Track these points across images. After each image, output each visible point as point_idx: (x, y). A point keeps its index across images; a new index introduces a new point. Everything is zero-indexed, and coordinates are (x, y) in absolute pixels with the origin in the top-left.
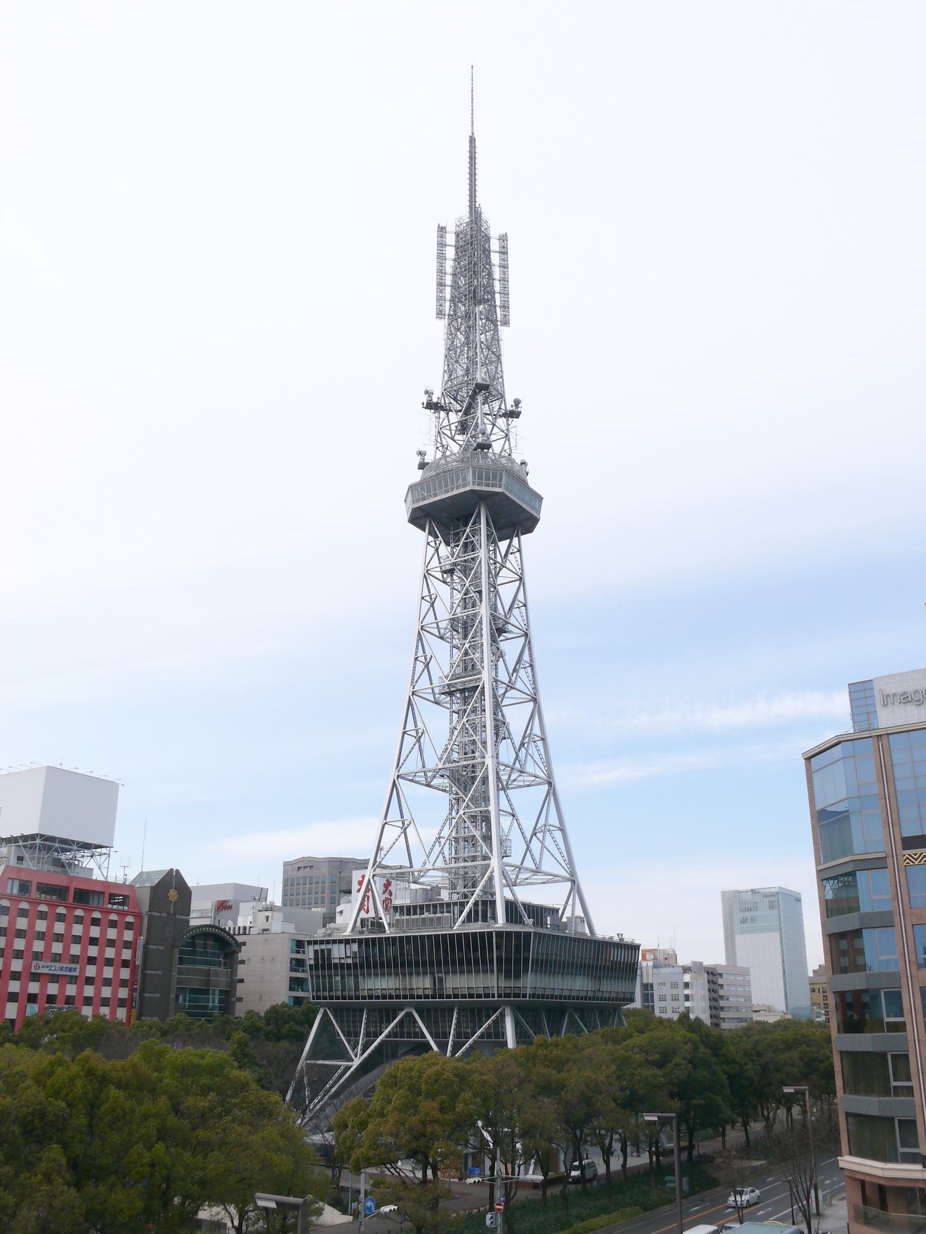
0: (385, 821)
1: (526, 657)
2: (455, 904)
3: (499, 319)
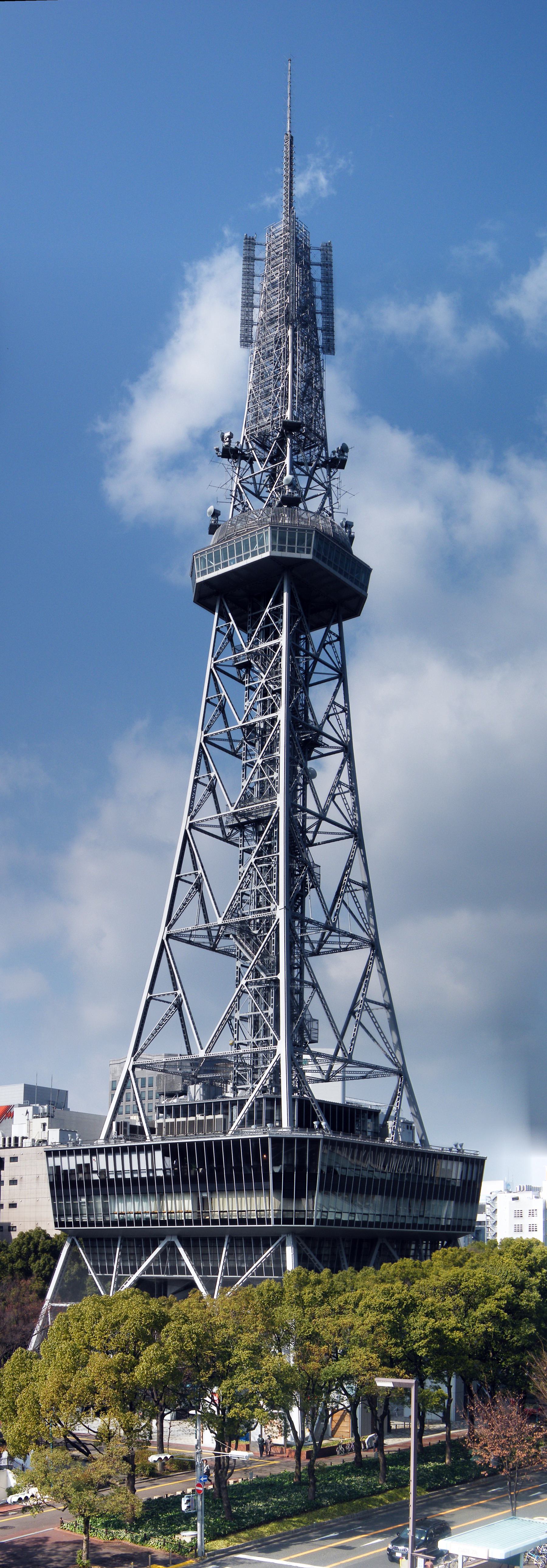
0: (149, 995)
3: (320, 344)
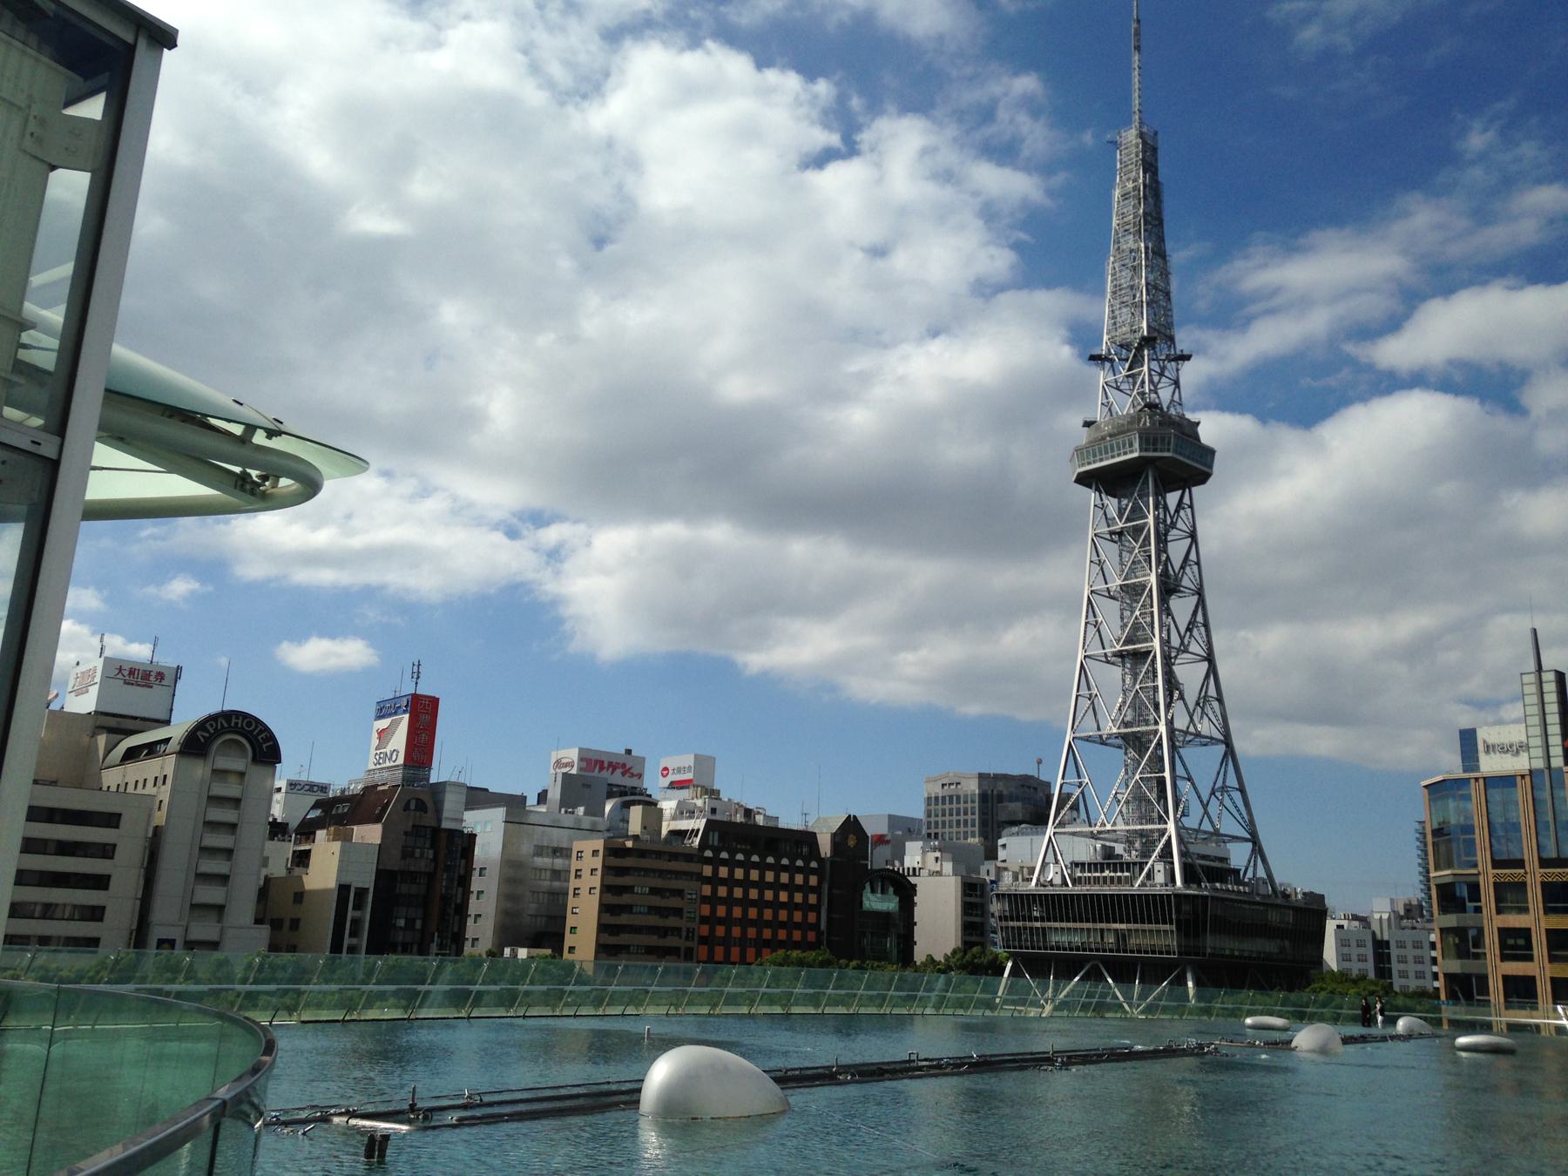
1: (1200, 618)
2: (1135, 864)
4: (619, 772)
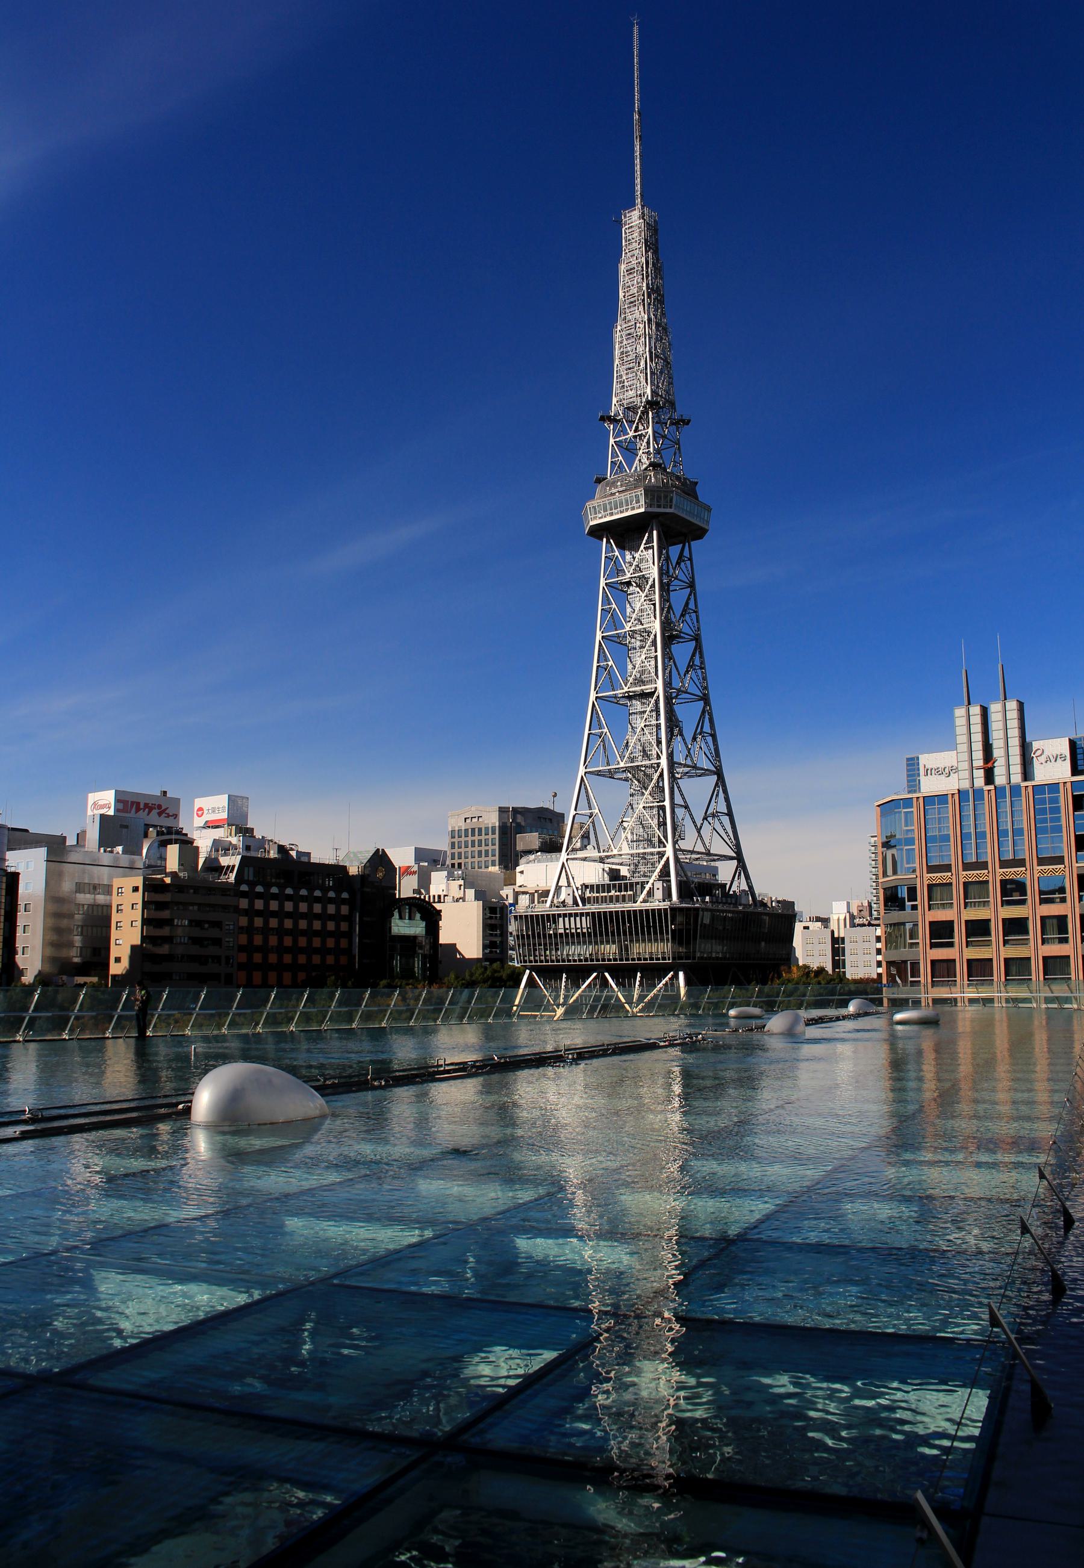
2: (637, 883)
4: (155, 812)
